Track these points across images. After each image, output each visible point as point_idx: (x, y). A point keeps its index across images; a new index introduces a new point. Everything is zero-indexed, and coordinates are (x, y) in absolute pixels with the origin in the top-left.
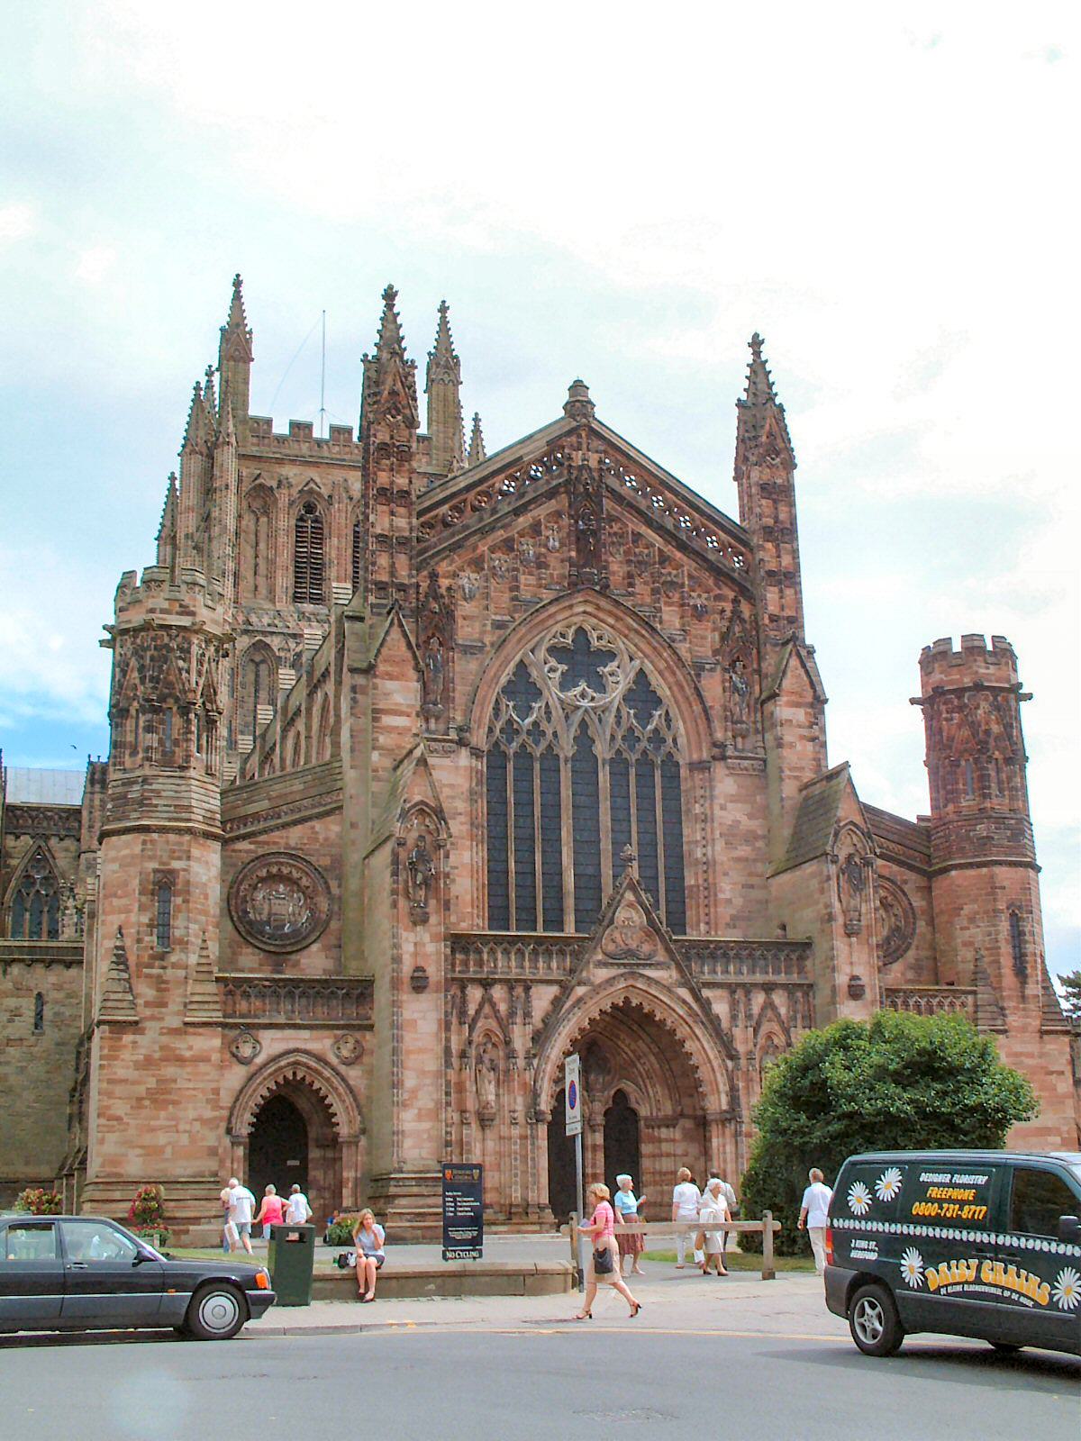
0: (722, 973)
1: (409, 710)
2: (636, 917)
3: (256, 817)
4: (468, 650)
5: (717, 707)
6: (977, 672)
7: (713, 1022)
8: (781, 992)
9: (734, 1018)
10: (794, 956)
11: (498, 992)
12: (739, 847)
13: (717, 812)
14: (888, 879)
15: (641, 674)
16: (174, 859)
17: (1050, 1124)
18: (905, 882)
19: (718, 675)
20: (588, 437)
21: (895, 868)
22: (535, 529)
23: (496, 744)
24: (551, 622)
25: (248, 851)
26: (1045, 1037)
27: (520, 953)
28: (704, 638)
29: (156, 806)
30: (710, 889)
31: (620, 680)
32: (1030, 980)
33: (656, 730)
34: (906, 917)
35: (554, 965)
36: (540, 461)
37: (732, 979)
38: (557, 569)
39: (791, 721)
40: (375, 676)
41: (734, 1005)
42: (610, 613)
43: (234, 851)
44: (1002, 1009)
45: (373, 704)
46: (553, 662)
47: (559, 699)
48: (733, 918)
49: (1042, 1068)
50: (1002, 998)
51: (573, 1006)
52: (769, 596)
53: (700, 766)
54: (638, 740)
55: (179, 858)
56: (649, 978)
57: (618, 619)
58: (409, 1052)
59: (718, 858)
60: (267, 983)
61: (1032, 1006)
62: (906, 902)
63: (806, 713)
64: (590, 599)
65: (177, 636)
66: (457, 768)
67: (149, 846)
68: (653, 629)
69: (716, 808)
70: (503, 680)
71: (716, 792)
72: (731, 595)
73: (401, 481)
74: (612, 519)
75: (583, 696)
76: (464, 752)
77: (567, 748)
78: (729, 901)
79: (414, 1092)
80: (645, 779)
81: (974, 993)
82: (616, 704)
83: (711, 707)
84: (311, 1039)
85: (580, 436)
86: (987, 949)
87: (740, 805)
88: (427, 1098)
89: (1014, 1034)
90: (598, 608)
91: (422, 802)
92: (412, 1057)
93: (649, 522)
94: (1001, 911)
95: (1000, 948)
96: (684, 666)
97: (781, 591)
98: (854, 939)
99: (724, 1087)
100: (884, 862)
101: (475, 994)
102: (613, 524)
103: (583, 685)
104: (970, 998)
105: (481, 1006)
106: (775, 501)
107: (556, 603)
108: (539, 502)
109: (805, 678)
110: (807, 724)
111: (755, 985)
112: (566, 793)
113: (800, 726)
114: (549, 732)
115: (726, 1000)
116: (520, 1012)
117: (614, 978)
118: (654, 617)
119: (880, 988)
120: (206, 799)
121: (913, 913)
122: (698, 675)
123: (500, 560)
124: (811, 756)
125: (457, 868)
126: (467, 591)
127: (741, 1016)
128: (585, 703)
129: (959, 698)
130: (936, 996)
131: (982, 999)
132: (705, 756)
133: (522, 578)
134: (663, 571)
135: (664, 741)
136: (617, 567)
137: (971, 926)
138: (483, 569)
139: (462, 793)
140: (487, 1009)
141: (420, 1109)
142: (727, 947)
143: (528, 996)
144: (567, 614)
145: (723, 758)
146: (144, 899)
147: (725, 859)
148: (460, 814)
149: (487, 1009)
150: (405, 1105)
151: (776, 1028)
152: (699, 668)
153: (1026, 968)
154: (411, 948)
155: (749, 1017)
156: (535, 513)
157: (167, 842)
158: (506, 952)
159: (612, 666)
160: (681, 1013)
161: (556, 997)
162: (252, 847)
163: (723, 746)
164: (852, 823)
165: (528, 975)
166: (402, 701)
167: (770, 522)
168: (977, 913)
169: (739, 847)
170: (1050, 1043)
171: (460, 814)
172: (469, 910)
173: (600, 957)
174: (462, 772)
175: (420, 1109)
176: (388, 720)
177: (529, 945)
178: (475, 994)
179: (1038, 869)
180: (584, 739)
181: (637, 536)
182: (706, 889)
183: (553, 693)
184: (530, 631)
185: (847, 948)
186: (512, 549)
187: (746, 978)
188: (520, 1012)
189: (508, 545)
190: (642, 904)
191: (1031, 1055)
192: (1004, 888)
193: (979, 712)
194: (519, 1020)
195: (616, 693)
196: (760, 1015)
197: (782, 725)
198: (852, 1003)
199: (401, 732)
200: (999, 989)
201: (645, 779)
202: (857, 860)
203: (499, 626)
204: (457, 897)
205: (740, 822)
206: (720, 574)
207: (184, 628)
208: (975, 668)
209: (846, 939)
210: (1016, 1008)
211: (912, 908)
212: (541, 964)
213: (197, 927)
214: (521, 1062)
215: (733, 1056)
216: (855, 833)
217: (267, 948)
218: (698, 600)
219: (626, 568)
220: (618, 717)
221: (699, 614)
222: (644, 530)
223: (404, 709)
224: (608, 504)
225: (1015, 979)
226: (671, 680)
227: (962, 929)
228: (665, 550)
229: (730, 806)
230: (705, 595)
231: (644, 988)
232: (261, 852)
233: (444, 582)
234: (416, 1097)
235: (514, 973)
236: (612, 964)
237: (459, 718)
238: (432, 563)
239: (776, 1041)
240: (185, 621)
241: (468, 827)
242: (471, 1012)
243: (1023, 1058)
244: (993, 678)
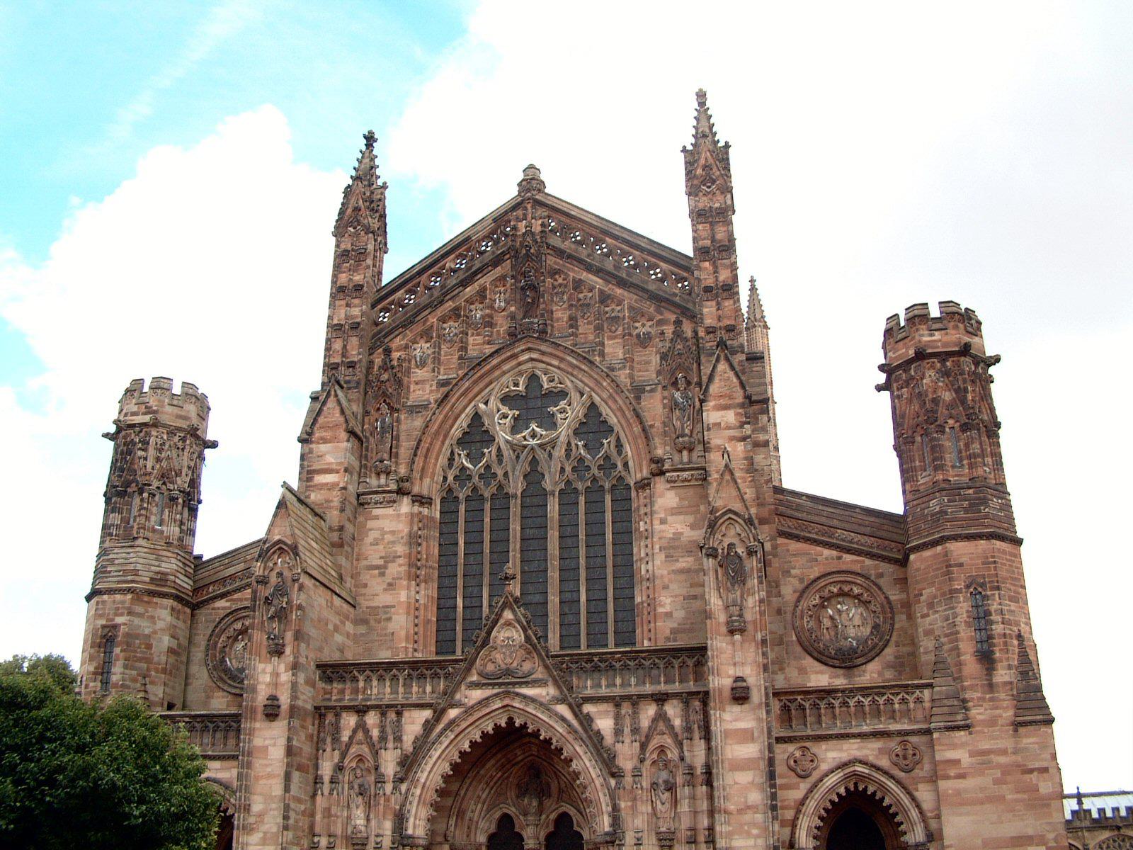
0: (607, 686)
1: (338, 468)
2: (516, 636)
3: (232, 577)
4: (415, 410)
5: (658, 424)
6: (920, 341)
7: (595, 740)
8: (675, 702)
9: (618, 732)
10: (690, 662)
11: (372, 719)
12: (681, 560)
13: (658, 527)
14: (859, 574)
15: (593, 406)
16: (116, 615)
17: (1030, 832)
18: (881, 575)
19: (658, 394)
20: (533, 207)
21: (868, 562)
22: (482, 295)
23: (450, 490)
24: (497, 373)
25: (224, 608)
26: (1022, 730)
27: (395, 678)
28: (648, 363)
29: (110, 572)
30: (652, 603)
31: (569, 414)
32: (999, 665)
33: (607, 458)
34: (883, 611)
35: (428, 689)
36: (488, 237)
37: (617, 691)
38: (502, 325)
39: (719, 424)
40: (312, 442)
41: (618, 718)
42: (551, 355)
43: (213, 609)
44: (964, 701)
45: (308, 466)
46: (504, 410)
47: (507, 441)
48: (673, 631)
49: (1019, 766)
50: (964, 689)
51: (445, 729)
52: (705, 310)
53: (643, 485)
54: (588, 468)
55: (122, 615)
56: (525, 697)
57: (562, 360)
58: (257, 778)
59: (658, 572)
60: (187, 719)
61: (1002, 696)
62: (882, 597)
63: (736, 414)
64: (530, 345)
65: (141, 431)
66: (399, 515)
67: (100, 606)
68: (591, 362)
69: (656, 522)
70: (456, 432)
71: (656, 508)
72: (673, 317)
73: (358, 278)
74: (554, 273)
75: (534, 436)
76: (406, 500)
77: (517, 486)
78: (669, 615)
79: (261, 815)
80: (595, 505)
81: (931, 686)
82: (563, 438)
83: (652, 426)
84: (222, 769)
85: (526, 209)
86: (946, 636)
87: (682, 517)
88: (272, 823)
89: (977, 729)
90: (543, 353)
91: (280, 541)
92: (261, 782)
93: (589, 268)
94: (959, 591)
95: (957, 632)
96: (622, 392)
97: (718, 304)
98: (737, 637)
99: (606, 808)
100: (854, 557)
101: (350, 720)
102: (557, 276)
103: (533, 426)
104: (927, 692)
105: (355, 731)
106: (711, 224)
107: (496, 355)
108: (485, 272)
109: (735, 380)
110: (738, 424)
111: (641, 697)
112: (515, 527)
113: (728, 428)
114: (500, 472)
115: (612, 714)
116: (391, 737)
117: (487, 699)
118: (593, 351)
119: (766, 688)
120: (157, 563)
121: (891, 608)
122: (638, 398)
123: (452, 327)
124: (742, 456)
125: (394, 606)
126: (418, 359)
127: (627, 730)
128: (532, 442)
129: (905, 371)
130: (883, 694)
131: (940, 692)
132: (645, 473)
133: (471, 340)
134: (607, 309)
135: (615, 466)
136: (561, 314)
137: (931, 612)
138: (432, 338)
139: (402, 538)
140: (360, 735)
141: (265, 833)
142: (613, 658)
143: (399, 721)
144: (514, 362)
145: (662, 473)
146: (92, 651)
147: (665, 572)
148: (400, 557)
149: (360, 735)
150: (248, 830)
151: (668, 741)
152: (639, 391)
153: (993, 651)
154: (267, 679)
155: (635, 731)
156: (482, 281)
157: (114, 602)
158: (381, 679)
159: (563, 404)
160: (561, 731)
161: (427, 721)
162: (228, 604)
163: (658, 461)
164: (730, 511)
165: (401, 699)
166: (333, 461)
167: (708, 243)
168: (935, 597)
169: (681, 560)
170: (1026, 736)
171: (400, 557)
172: (404, 645)
173: (475, 678)
174: (403, 518)
175: (265, 833)
176: (320, 479)
177: (404, 670)
178: (350, 720)
179: (1019, 542)
180: (533, 475)
181: (578, 284)
182: (649, 605)
183: (503, 436)
184: (475, 382)
185: (730, 647)
186: (459, 316)
187: (633, 690)
188: (391, 737)
189: (456, 313)
190: (519, 622)
191: (1004, 752)
192: (961, 565)
193: (925, 381)
194: (390, 745)
195: (564, 430)
196: (650, 728)
197: (709, 429)
198: (737, 709)
199: (330, 487)
200: (959, 679)
201: (595, 505)
202: (740, 550)
203: (443, 384)
204: (393, 634)
205: (681, 534)
206: (660, 300)
207: (145, 425)
208: (917, 337)
209: (729, 638)
210: (983, 699)
211: (889, 602)
212: (415, 689)
213: (134, 672)
214: (389, 787)
215: (616, 774)
216: (737, 521)
217: (234, 691)
218: (643, 328)
219: (569, 313)
220: (568, 450)
221: (644, 341)
222: (584, 275)
223: (334, 467)
224: (552, 261)
225: (978, 666)
226: (614, 407)
227: (923, 616)
228: (606, 289)
229: (669, 518)
230: (650, 323)
231: (521, 707)
232: (234, 607)
233: (395, 355)
234: (262, 822)
235: (388, 697)
236: (484, 684)
237: (403, 470)
238: (386, 340)
239: (670, 755)
240: (147, 419)
241: (406, 568)
242: (345, 738)
243: (992, 756)
244: (939, 344)
